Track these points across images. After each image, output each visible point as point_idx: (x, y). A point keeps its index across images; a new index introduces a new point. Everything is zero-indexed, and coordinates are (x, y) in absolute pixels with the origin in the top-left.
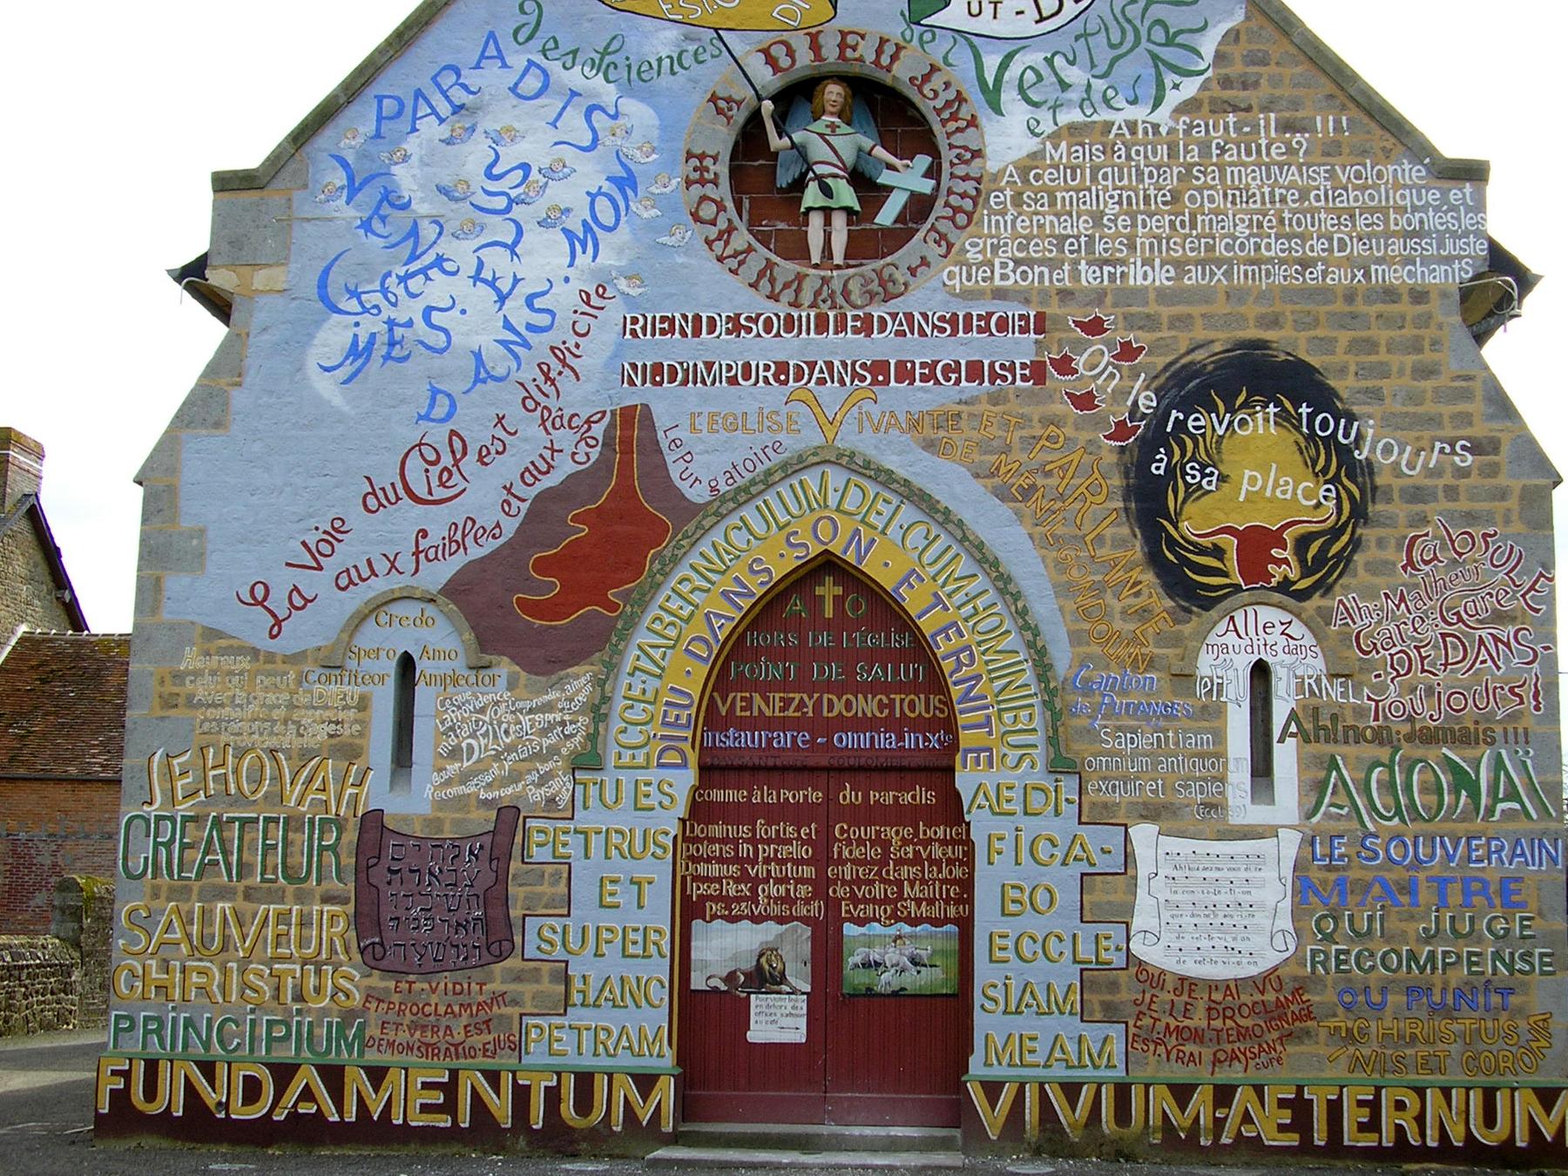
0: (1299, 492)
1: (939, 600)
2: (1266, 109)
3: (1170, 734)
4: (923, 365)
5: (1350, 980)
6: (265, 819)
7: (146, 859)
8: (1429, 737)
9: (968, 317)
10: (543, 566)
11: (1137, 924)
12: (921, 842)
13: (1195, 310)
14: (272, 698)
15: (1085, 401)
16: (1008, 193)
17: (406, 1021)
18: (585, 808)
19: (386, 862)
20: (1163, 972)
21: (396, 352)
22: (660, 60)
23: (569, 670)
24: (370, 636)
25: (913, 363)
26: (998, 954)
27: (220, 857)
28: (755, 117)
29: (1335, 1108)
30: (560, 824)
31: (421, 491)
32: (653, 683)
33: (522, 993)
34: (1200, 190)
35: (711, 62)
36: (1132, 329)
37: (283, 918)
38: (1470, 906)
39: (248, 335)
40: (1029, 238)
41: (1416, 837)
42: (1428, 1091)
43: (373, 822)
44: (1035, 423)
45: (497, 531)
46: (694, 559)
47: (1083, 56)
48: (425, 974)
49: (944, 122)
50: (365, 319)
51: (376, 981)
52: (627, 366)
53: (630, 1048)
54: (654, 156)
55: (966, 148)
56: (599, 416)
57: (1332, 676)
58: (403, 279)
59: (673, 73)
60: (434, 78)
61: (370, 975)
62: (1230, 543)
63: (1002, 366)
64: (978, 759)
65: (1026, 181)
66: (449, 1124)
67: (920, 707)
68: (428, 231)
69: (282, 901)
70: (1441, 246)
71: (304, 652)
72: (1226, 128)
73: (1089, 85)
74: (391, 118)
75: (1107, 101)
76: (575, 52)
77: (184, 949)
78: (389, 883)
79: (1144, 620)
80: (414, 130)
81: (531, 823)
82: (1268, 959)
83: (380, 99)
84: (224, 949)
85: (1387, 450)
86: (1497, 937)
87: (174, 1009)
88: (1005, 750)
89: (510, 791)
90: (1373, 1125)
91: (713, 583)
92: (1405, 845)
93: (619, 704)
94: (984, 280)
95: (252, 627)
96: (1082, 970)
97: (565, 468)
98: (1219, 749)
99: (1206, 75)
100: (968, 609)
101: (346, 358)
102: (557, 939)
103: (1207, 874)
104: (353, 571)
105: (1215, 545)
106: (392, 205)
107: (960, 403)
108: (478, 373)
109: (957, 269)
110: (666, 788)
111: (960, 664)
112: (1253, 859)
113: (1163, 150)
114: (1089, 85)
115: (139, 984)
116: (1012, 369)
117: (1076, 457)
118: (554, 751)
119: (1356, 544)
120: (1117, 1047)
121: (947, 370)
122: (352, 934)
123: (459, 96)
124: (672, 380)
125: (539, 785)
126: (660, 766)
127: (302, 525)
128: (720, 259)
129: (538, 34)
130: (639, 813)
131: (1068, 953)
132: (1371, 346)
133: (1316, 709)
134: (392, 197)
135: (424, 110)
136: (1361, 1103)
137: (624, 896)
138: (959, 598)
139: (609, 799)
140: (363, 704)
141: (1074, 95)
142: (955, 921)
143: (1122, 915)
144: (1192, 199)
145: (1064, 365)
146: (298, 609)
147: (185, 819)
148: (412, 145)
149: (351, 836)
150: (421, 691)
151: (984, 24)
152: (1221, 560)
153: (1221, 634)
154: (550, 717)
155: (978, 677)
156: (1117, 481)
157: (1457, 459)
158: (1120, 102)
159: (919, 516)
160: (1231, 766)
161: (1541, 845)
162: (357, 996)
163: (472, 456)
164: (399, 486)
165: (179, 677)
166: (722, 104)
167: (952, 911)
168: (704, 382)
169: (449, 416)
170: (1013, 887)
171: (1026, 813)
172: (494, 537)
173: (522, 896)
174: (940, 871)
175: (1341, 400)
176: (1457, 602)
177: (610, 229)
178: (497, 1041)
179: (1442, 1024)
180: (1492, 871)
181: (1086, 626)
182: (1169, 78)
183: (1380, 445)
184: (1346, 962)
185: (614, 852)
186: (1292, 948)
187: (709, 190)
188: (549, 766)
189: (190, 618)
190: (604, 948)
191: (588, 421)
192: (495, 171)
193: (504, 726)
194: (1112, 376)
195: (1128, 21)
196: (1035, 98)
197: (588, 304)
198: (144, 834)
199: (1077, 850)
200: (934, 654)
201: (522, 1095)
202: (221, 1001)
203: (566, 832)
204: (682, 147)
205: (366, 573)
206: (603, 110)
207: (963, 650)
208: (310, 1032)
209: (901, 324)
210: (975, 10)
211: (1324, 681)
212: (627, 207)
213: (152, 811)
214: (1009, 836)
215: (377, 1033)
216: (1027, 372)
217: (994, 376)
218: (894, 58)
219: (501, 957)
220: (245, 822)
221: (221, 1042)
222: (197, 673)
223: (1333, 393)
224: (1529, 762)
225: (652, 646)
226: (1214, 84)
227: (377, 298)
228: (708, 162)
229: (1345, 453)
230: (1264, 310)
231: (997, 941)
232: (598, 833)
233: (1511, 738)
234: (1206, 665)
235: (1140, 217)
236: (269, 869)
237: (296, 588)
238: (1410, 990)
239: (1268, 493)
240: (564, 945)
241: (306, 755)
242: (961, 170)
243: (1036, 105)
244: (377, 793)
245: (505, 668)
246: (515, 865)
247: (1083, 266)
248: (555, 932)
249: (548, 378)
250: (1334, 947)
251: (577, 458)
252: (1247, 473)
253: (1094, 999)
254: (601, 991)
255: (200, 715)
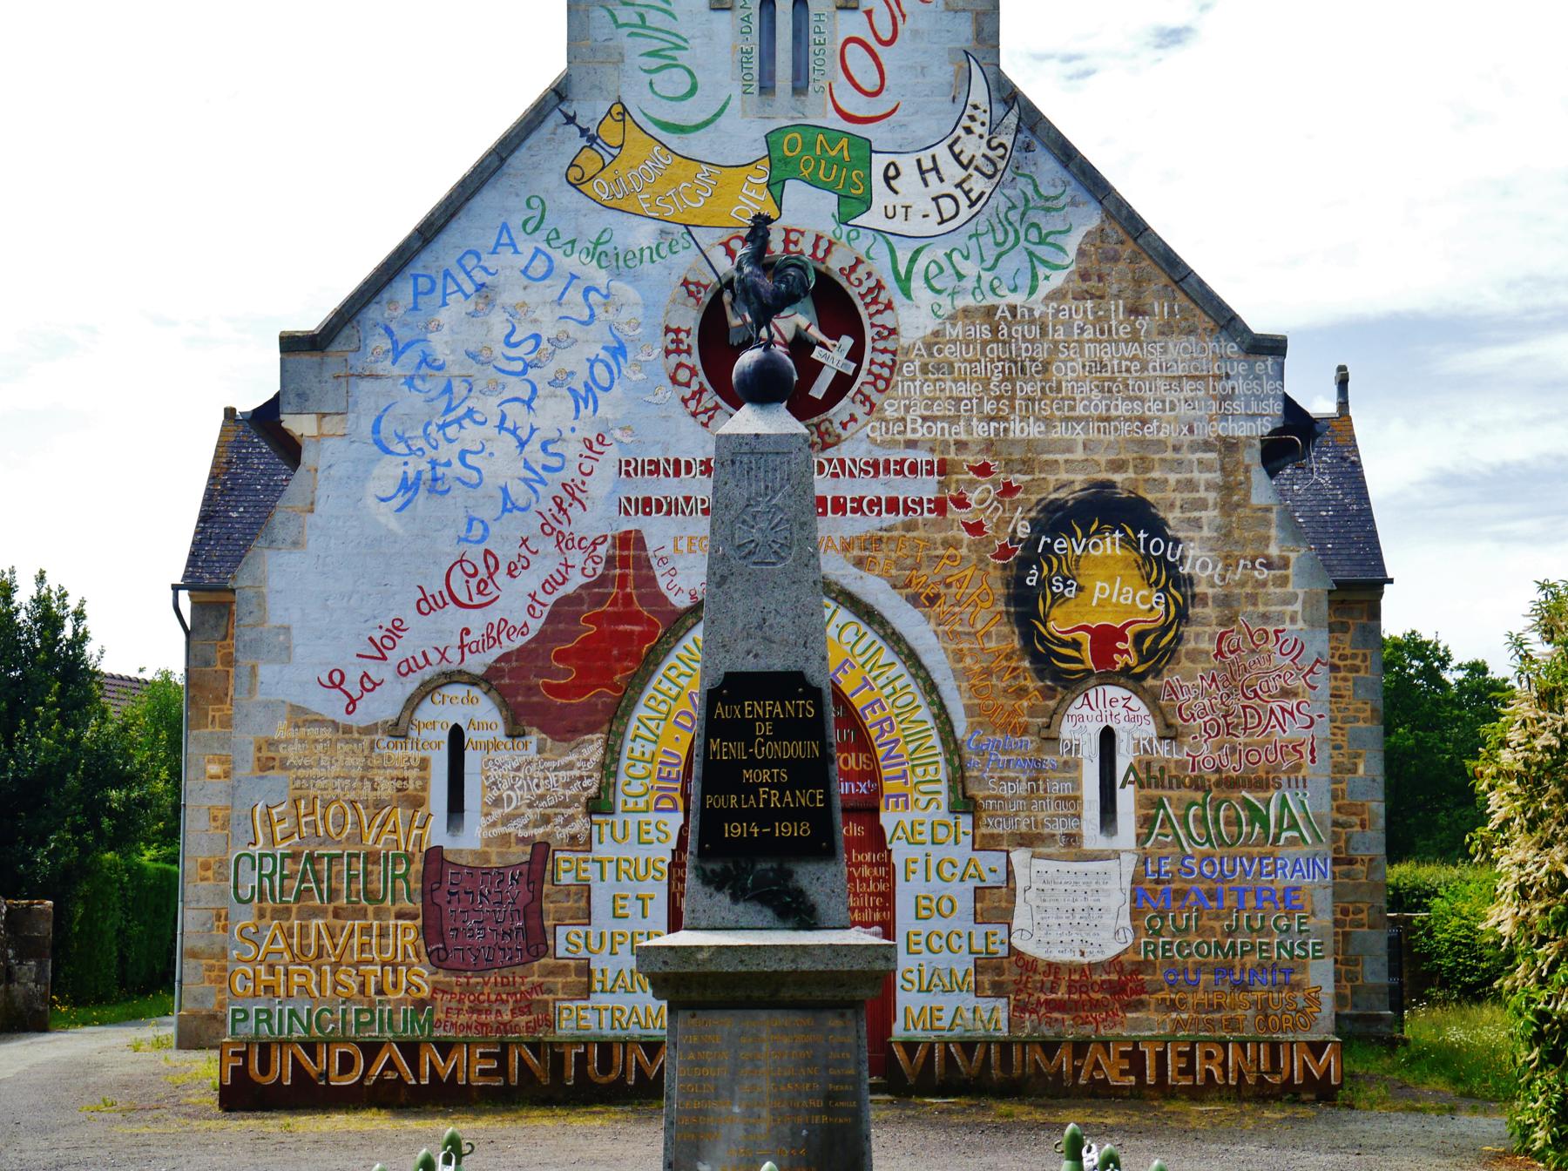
0: (1137, 598)
1: (866, 683)
2: (1118, 296)
3: (1041, 783)
4: (853, 500)
5: (1173, 963)
6: (349, 855)
7: (253, 888)
8: (1233, 784)
9: (887, 462)
10: (560, 656)
11: (1016, 924)
12: (853, 865)
13: (1060, 457)
14: (350, 761)
15: (976, 528)
16: (917, 363)
17: (466, 1007)
18: (600, 842)
19: (447, 886)
20: (1035, 960)
21: (440, 486)
22: (642, 250)
23: (586, 737)
24: (426, 712)
25: (845, 499)
26: (914, 948)
27: (313, 885)
28: (718, 296)
29: (1161, 1058)
30: (581, 856)
31: (464, 598)
32: (650, 748)
33: (556, 983)
34: (1064, 362)
35: (682, 253)
36: (1012, 472)
37: (366, 931)
38: (1261, 908)
39: (316, 470)
40: (933, 399)
41: (1222, 858)
42: (1230, 1045)
43: (435, 856)
44: (938, 545)
45: (525, 630)
46: (679, 650)
47: (974, 253)
48: (479, 971)
49: (867, 305)
50: (411, 459)
51: (441, 976)
52: (623, 500)
53: (639, 1023)
54: (639, 330)
55: (883, 326)
56: (602, 539)
57: (1161, 738)
58: (442, 427)
59: (653, 262)
60: (459, 261)
61: (436, 973)
62: (1085, 638)
63: (913, 501)
64: (897, 802)
65: (931, 355)
66: (502, 1083)
67: (852, 762)
68: (460, 388)
69: (365, 917)
70: (1247, 406)
71: (376, 724)
72: (1085, 312)
73: (979, 277)
74: (426, 294)
75: (993, 290)
76: (573, 242)
77: (287, 957)
78: (449, 902)
79: (1020, 697)
80: (445, 304)
81: (558, 855)
82: (1112, 950)
83: (415, 277)
84: (319, 956)
85: (1204, 566)
86: (1281, 932)
87: (280, 1003)
88: (916, 796)
89: (541, 830)
90: (1189, 1070)
91: (694, 670)
92: (1214, 864)
93: (624, 763)
94: (899, 433)
95: (331, 705)
96: (976, 959)
97: (576, 581)
98: (1078, 794)
99: (1071, 269)
100: (888, 690)
101: (399, 491)
102: (581, 942)
103: (1068, 887)
104: (411, 661)
105: (1074, 640)
106: (429, 365)
107: (881, 530)
108: (505, 504)
109: (878, 425)
110: (662, 827)
111: (883, 732)
112: (1102, 875)
113: (1036, 330)
114: (979, 277)
115: (250, 984)
116: (920, 503)
117: (969, 573)
118: (575, 799)
119: (1179, 638)
120: (1003, 1016)
121: (871, 503)
122: (421, 942)
123: (480, 276)
124: (659, 510)
125: (564, 826)
126: (657, 810)
127: (370, 624)
128: (694, 415)
129: (543, 226)
130: (642, 846)
131: (965, 947)
132: (1190, 485)
133: (1149, 764)
134: (430, 359)
135: (452, 287)
136: (1180, 1054)
137: (633, 908)
138: (882, 681)
139: (619, 834)
140: (424, 764)
141: (969, 283)
142: (879, 924)
143: (1004, 916)
144: (1059, 369)
145: (961, 503)
146: (368, 691)
147: (284, 856)
148: (444, 316)
149: (418, 866)
150: (470, 756)
151: (896, 225)
152: (1079, 650)
153: (1077, 707)
154: (569, 773)
155: (897, 741)
156: (1000, 589)
157: (1256, 573)
158: (1003, 291)
159: (851, 618)
160: (1085, 805)
161: (1314, 863)
162: (426, 989)
163: (503, 568)
164: (446, 594)
165: (272, 744)
166: (693, 288)
167: (877, 916)
168: (683, 512)
169: (483, 539)
170: (924, 898)
171: (933, 843)
172: (523, 634)
173: (552, 910)
174: (868, 886)
175: (1169, 527)
176: (1254, 682)
177: (607, 389)
178: (536, 1021)
179: (1241, 997)
180: (1281, 882)
181: (976, 701)
182: (1042, 271)
183: (1198, 563)
184: (1170, 950)
185: (623, 876)
186: (1130, 941)
187: (684, 358)
188: (570, 811)
189: (282, 698)
190: (618, 948)
191: (594, 543)
192: (513, 340)
193: (536, 781)
194: (997, 509)
195: (1011, 224)
196: (937, 284)
197: (590, 448)
198: (250, 866)
199: (971, 870)
200: (864, 724)
201: (558, 1061)
202: (317, 994)
203: (585, 861)
204: (661, 321)
205: (421, 662)
206: (597, 290)
207: (885, 720)
208: (390, 1018)
209: (835, 468)
210: (890, 214)
211: (1155, 742)
212: (620, 372)
213: (256, 850)
214: (922, 861)
215: (442, 1016)
216: (932, 506)
217: (907, 509)
218: (828, 251)
219: (538, 957)
220: (332, 858)
221: (319, 1027)
222: (288, 741)
223: (1164, 523)
224: (1306, 802)
225: (648, 719)
226: (1076, 277)
227: (420, 443)
228: (682, 336)
229: (1172, 567)
230: (1113, 457)
231: (913, 938)
232: (610, 861)
233: (1293, 783)
234: (1067, 730)
235: (1018, 384)
236: (354, 893)
237: (366, 675)
238: (1216, 972)
239: (1114, 600)
240: (587, 947)
241: (379, 805)
242: (880, 345)
243: (939, 292)
244: (437, 833)
245: (534, 737)
246: (546, 888)
247: (975, 422)
248: (579, 937)
249: (560, 508)
250: (1161, 940)
251: (586, 572)
252: (1099, 584)
253: (986, 979)
254: (616, 981)
255: (292, 774)
